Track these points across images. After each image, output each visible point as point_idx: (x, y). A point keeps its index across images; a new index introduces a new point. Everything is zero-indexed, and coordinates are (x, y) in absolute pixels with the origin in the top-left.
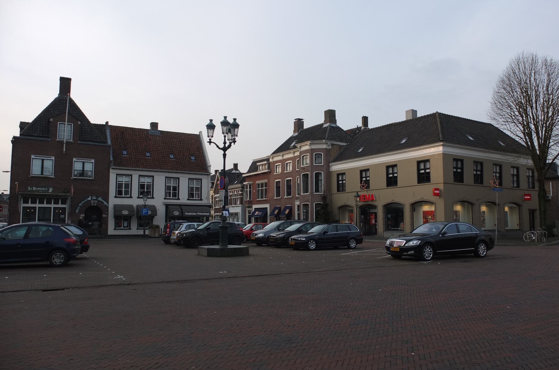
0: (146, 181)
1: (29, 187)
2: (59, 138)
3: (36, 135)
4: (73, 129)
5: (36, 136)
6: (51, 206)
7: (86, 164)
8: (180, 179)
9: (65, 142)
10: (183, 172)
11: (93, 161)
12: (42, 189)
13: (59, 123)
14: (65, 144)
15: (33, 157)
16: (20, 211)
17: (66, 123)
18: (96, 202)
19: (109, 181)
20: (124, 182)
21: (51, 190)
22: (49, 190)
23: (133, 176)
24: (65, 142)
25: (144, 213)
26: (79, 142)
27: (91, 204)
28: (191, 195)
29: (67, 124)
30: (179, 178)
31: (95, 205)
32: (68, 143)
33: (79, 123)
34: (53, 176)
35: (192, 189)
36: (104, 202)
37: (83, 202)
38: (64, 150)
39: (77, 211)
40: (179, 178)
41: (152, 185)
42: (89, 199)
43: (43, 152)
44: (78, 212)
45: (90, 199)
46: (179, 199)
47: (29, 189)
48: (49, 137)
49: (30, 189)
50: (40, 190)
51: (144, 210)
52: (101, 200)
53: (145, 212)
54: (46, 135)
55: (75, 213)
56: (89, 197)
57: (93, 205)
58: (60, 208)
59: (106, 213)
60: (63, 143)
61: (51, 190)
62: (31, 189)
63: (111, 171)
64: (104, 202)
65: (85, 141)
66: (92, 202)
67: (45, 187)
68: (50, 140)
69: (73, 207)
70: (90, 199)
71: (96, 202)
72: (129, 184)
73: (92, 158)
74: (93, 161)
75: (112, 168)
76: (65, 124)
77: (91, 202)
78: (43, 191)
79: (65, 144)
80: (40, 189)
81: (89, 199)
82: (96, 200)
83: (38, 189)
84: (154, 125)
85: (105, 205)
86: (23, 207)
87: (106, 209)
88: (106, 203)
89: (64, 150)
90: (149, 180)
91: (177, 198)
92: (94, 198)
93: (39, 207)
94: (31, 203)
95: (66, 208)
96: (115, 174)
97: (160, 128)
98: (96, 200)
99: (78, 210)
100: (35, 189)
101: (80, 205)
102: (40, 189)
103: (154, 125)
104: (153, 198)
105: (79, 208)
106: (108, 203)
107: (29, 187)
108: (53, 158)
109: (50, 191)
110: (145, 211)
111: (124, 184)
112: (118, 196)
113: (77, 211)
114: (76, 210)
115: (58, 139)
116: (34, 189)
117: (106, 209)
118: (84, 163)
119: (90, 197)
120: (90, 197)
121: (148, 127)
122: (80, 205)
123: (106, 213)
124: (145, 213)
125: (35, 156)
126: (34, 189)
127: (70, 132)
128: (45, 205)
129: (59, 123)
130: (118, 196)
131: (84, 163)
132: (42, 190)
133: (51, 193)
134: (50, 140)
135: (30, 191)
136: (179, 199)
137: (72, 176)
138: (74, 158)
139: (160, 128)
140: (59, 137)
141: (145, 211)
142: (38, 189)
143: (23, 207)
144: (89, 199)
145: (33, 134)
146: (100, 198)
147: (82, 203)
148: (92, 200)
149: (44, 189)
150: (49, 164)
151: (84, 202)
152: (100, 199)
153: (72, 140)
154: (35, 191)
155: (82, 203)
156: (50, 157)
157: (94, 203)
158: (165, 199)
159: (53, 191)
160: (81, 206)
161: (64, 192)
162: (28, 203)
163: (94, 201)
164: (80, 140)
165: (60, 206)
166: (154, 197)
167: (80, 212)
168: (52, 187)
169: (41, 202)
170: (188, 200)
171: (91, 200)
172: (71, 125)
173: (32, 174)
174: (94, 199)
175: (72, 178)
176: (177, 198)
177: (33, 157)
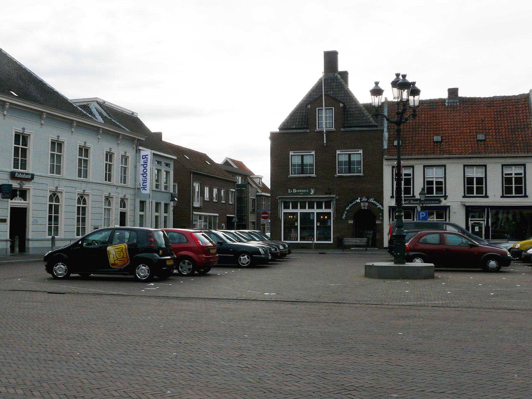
0: (434, 174)
1: (289, 190)
2: (333, 128)
3: (294, 127)
4: (334, 114)
5: (295, 129)
6: (313, 212)
7: (352, 156)
8: (487, 166)
9: (325, 132)
10: (503, 155)
11: (361, 152)
12: (303, 191)
13: (318, 109)
14: (325, 134)
15: (291, 153)
16: (280, 218)
17: (324, 108)
18: (367, 204)
19: (382, 176)
20: (513, 176)
21: (313, 191)
22: (310, 191)
23: (415, 167)
24: (325, 132)
25: (421, 218)
26: (342, 129)
27: (361, 207)
28: (507, 191)
29: (325, 109)
30: (486, 165)
31: (366, 208)
32: (327, 132)
33: (341, 105)
34: (314, 175)
35: (470, 181)
36: (377, 204)
37: (350, 205)
38: (325, 142)
39: (344, 216)
40: (486, 165)
41: (484, 179)
42: (358, 201)
43: (300, 146)
44: (345, 218)
45: (360, 202)
46: (486, 196)
47: (289, 192)
48: (307, 128)
49: (290, 191)
50: (301, 192)
51: (421, 213)
52: (373, 201)
53: (423, 216)
54: (306, 126)
55: (342, 219)
56: (357, 199)
57: (363, 208)
58: (324, 214)
59: (381, 218)
60: (323, 133)
61: (313, 191)
62: (291, 191)
63: (385, 163)
64: (377, 204)
65: (351, 127)
66: (362, 204)
67: (306, 189)
68: (308, 131)
69: (339, 211)
70: (360, 202)
71: (367, 204)
72: (411, 178)
73: (360, 148)
74: (361, 152)
75: (385, 159)
76: (323, 109)
77: (360, 205)
78: (305, 194)
79: (325, 134)
80: (301, 191)
81: (357, 201)
82: (367, 201)
83: (299, 191)
84: (453, 92)
85: (379, 208)
86: (284, 213)
87: (381, 214)
88: (380, 206)
89: (325, 142)
90: (520, 170)
91: (484, 195)
92: (364, 199)
93: (300, 213)
94: (309, 208)
95: (330, 213)
96: (391, 167)
97: (461, 94)
98: (367, 201)
99: (344, 215)
100: (295, 192)
101: (347, 209)
102: (301, 191)
103: (453, 92)
104: (526, 196)
105: (346, 212)
106: (382, 206)
107: (289, 190)
108: (313, 153)
109: (311, 193)
110: (423, 214)
111: (513, 179)
112: (506, 195)
113: (344, 216)
114: (342, 215)
115: (317, 129)
116: (295, 191)
117: (381, 214)
118: (302, 156)
119: (359, 198)
120: (359, 198)
121: (445, 95)
122: (347, 209)
123: (381, 218)
124: (422, 217)
125: (294, 153)
126: (295, 191)
127: (332, 117)
128: (307, 210)
129: (317, 109)
130: (506, 195)
131: (302, 156)
132: (303, 192)
133: (313, 195)
134: (308, 131)
135: (290, 194)
136: (486, 196)
137: (336, 174)
138: (337, 151)
139: (461, 94)
140: (318, 127)
141: (423, 214)
142: (299, 191)
143: (284, 213)
144: (358, 201)
145: (291, 127)
146: (371, 200)
147: (349, 207)
148: (361, 202)
149: (305, 191)
150: (310, 159)
151: (351, 205)
152: (371, 200)
153: (334, 128)
154: (295, 194)
155: (349, 207)
156: (311, 152)
157: (364, 206)
158: (464, 197)
159: (315, 194)
160: (348, 209)
161: (326, 194)
162: (289, 208)
163: (364, 204)
164: (344, 127)
165: (324, 210)
166: (527, 194)
167: (347, 219)
168: (314, 188)
169: (303, 207)
170: (503, 197)
171: (360, 203)
172: (332, 109)
173: (291, 174)
174: (364, 201)
175: (335, 176)
176: (484, 195)
177: (291, 153)
